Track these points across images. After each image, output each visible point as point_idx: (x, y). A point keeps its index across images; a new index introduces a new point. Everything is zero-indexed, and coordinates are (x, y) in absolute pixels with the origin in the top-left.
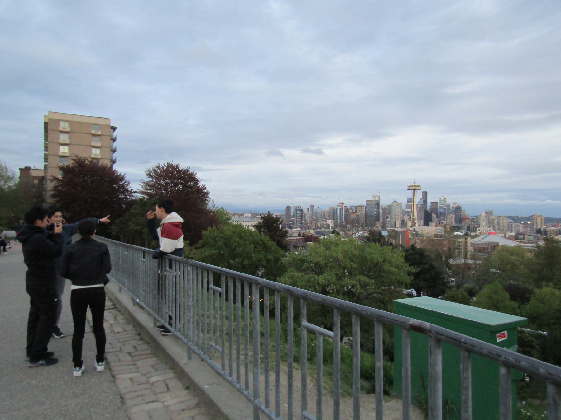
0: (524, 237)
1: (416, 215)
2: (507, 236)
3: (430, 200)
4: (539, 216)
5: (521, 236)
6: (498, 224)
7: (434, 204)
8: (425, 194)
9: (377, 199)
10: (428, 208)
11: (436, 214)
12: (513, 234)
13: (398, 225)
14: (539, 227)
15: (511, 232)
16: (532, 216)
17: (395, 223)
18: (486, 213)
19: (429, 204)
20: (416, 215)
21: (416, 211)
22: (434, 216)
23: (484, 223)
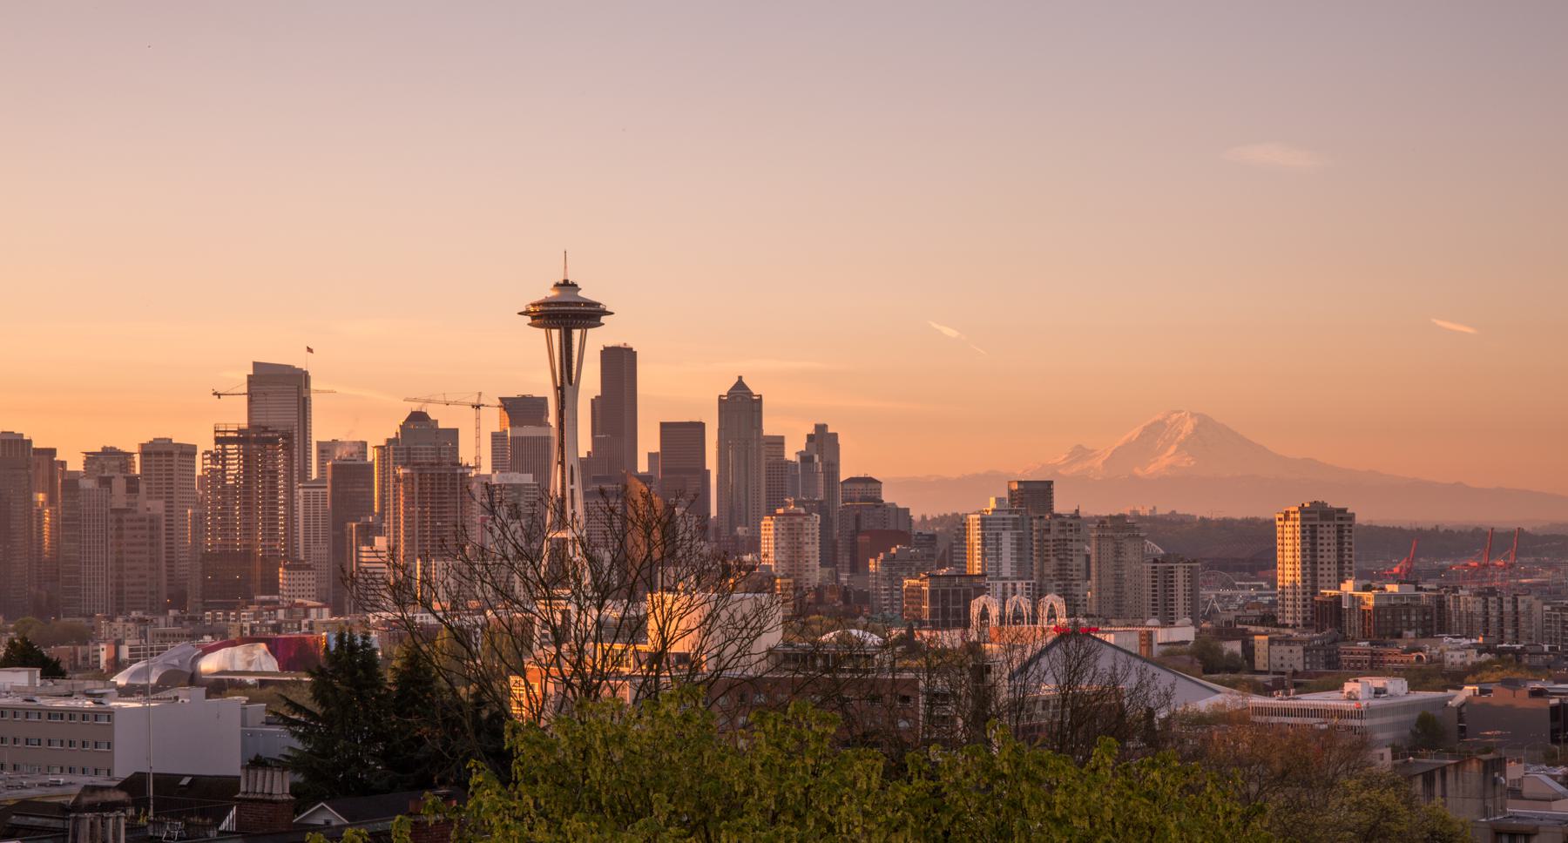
0: (1249, 650)
2: (1157, 650)
5: (1235, 647)
7: (682, 437)
8: (619, 363)
10: (643, 467)
12: (1184, 632)
15: (1168, 621)
19: (648, 442)
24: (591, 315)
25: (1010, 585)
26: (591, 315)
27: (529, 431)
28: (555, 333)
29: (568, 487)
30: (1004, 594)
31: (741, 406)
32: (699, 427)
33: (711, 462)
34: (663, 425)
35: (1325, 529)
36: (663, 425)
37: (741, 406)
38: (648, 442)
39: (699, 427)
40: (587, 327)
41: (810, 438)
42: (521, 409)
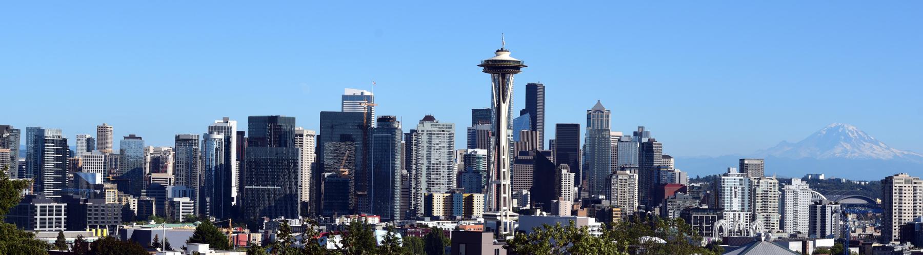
1: (506, 170)
3: (555, 114)
4: (907, 181)
6: (782, 210)
7: (567, 132)
8: (533, 93)
9: (362, 108)
11: (574, 168)
13: (438, 209)
14: (908, 218)
15: (823, 236)
16: (888, 183)
17: (429, 200)
18: (743, 168)
20: (506, 170)
21: (506, 157)
22: (567, 177)
23: (736, 204)
24: (515, 67)
25: (737, 214)
26: (515, 67)
27: (487, 127)
28: (496, 75)
29: (502, 157)
30: (734, 219)
31: (597, 116)
32: (576, 127)
33: (581, 147)
34: (558, 126)
35: (907, 188)
36: (558, 126)
37: (597, 116)
38: (550, 134)
39: (576, 127)
40: (513, 73)
41: (635, 134)
42: (479, 116)
